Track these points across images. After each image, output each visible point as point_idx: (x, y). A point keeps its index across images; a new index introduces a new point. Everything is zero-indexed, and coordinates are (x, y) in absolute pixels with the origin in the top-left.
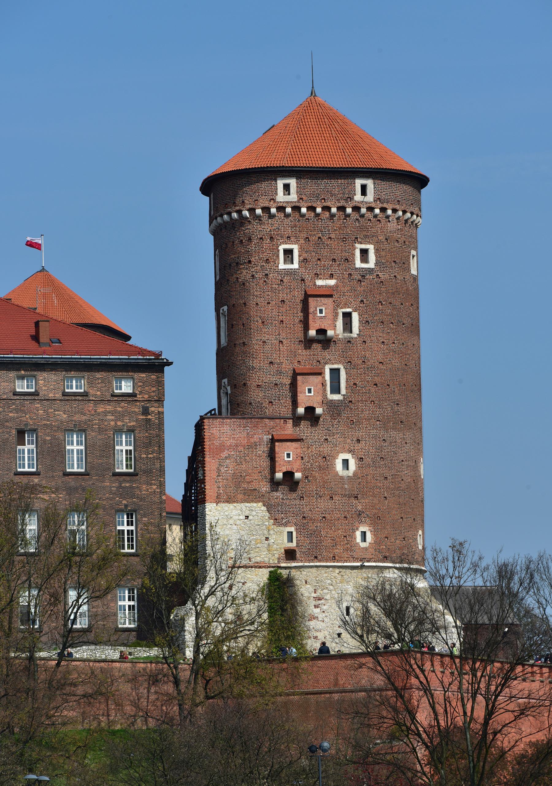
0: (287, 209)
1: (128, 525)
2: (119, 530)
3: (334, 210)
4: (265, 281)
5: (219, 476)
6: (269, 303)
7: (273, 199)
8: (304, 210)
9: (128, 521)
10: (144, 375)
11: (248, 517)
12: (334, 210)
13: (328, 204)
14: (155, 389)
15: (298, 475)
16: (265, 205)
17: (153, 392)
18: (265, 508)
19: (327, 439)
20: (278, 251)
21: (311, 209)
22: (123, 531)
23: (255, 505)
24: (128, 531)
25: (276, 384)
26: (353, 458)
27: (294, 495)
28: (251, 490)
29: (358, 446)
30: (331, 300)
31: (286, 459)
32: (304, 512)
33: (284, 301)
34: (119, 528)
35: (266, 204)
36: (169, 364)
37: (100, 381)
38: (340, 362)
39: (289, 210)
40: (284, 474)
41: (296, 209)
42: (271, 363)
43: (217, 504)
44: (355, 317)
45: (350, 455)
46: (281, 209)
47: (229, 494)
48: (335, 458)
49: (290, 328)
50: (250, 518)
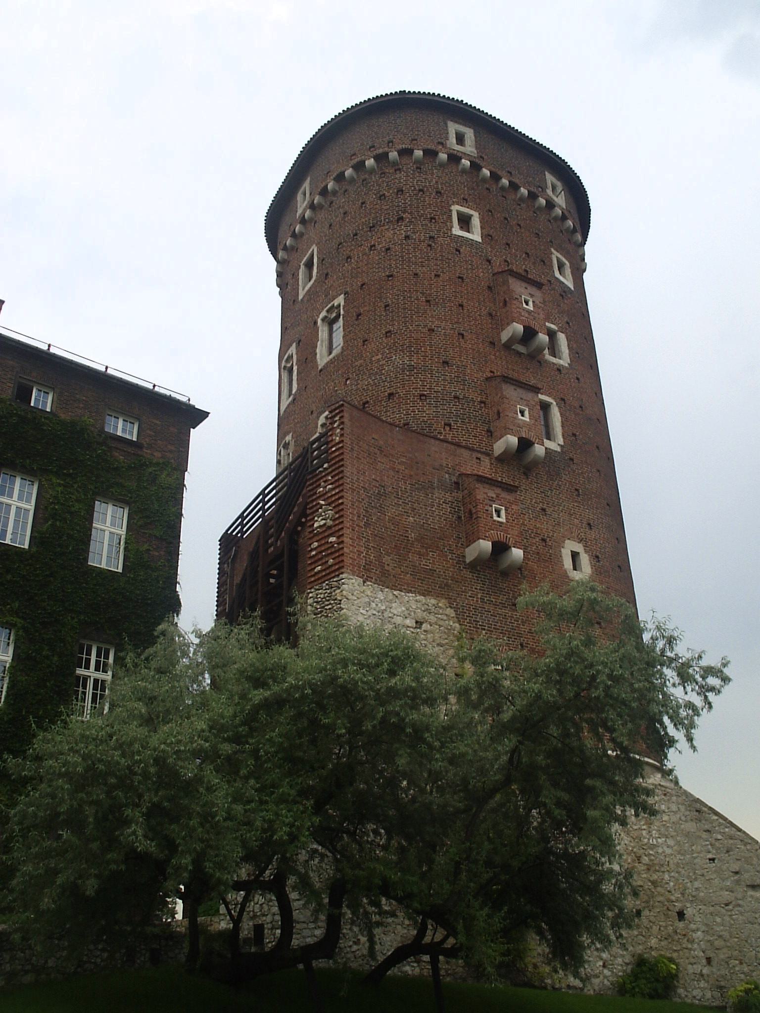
0: (463, 160)
1: (97, 669)
2: (78, 677)
3: (524, 191)
4: (430, 246)
5: (367, 525)
6: (437, 276)
7: (442, 144)
8: (486, 172)
9: (98, 663)
10: (158, 422)
11: (421, 623)
12: (524, 191)
13: (517, 181)
14: (173, 448)
15: (517, 553)
16: (429, 147)
17: (171, 451)
18: (451, 612)
19: (544, 510)
20: (451, 211)
21: (496, 177)
22: (86, 679)
23: (433, 601)
24: (96, 681)
25: (456, 397)
26: (586, 552)
27: (502, 598)
28: (425, 571)
29: (592, 534)
30: (538, 293)
31: (495, 518)
32: (520, 635)
33: (462, 278)
34: (80, 672)
35: (431, 146)
36: (203, 415)
37: (81, 405)
38: (549, 395)
39: (466, 163)
40: (494, 544)
41: (476, 167)
42: (445, 363)
43: (364, 582)
44: (562, 338)
45: (581, 545)
46: (454, 158)
47: (386, 567)
48: (560, 545)
49: (475, 319)
50: (425, 626)
